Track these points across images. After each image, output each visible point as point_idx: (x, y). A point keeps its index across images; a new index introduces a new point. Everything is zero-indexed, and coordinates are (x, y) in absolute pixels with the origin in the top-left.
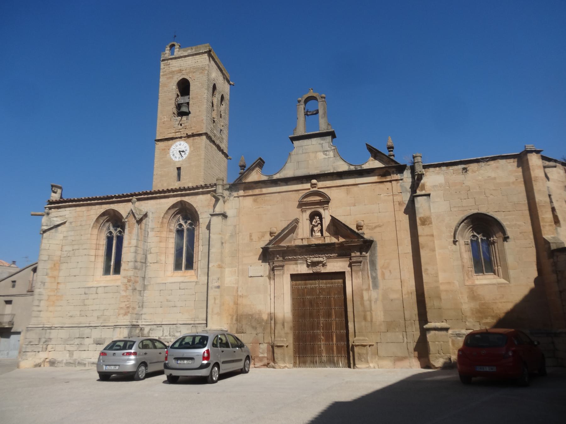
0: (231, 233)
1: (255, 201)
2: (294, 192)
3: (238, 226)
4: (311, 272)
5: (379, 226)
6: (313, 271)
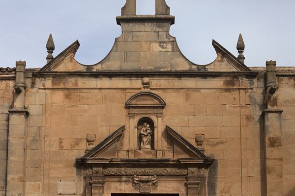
0: (34, 137)
1: (67, 96)
2: (119, 91)
3: (43, 128)
4: (138, 192)
5: (222, 143)
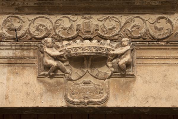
4: (59, 102)
6: (67, 100)
